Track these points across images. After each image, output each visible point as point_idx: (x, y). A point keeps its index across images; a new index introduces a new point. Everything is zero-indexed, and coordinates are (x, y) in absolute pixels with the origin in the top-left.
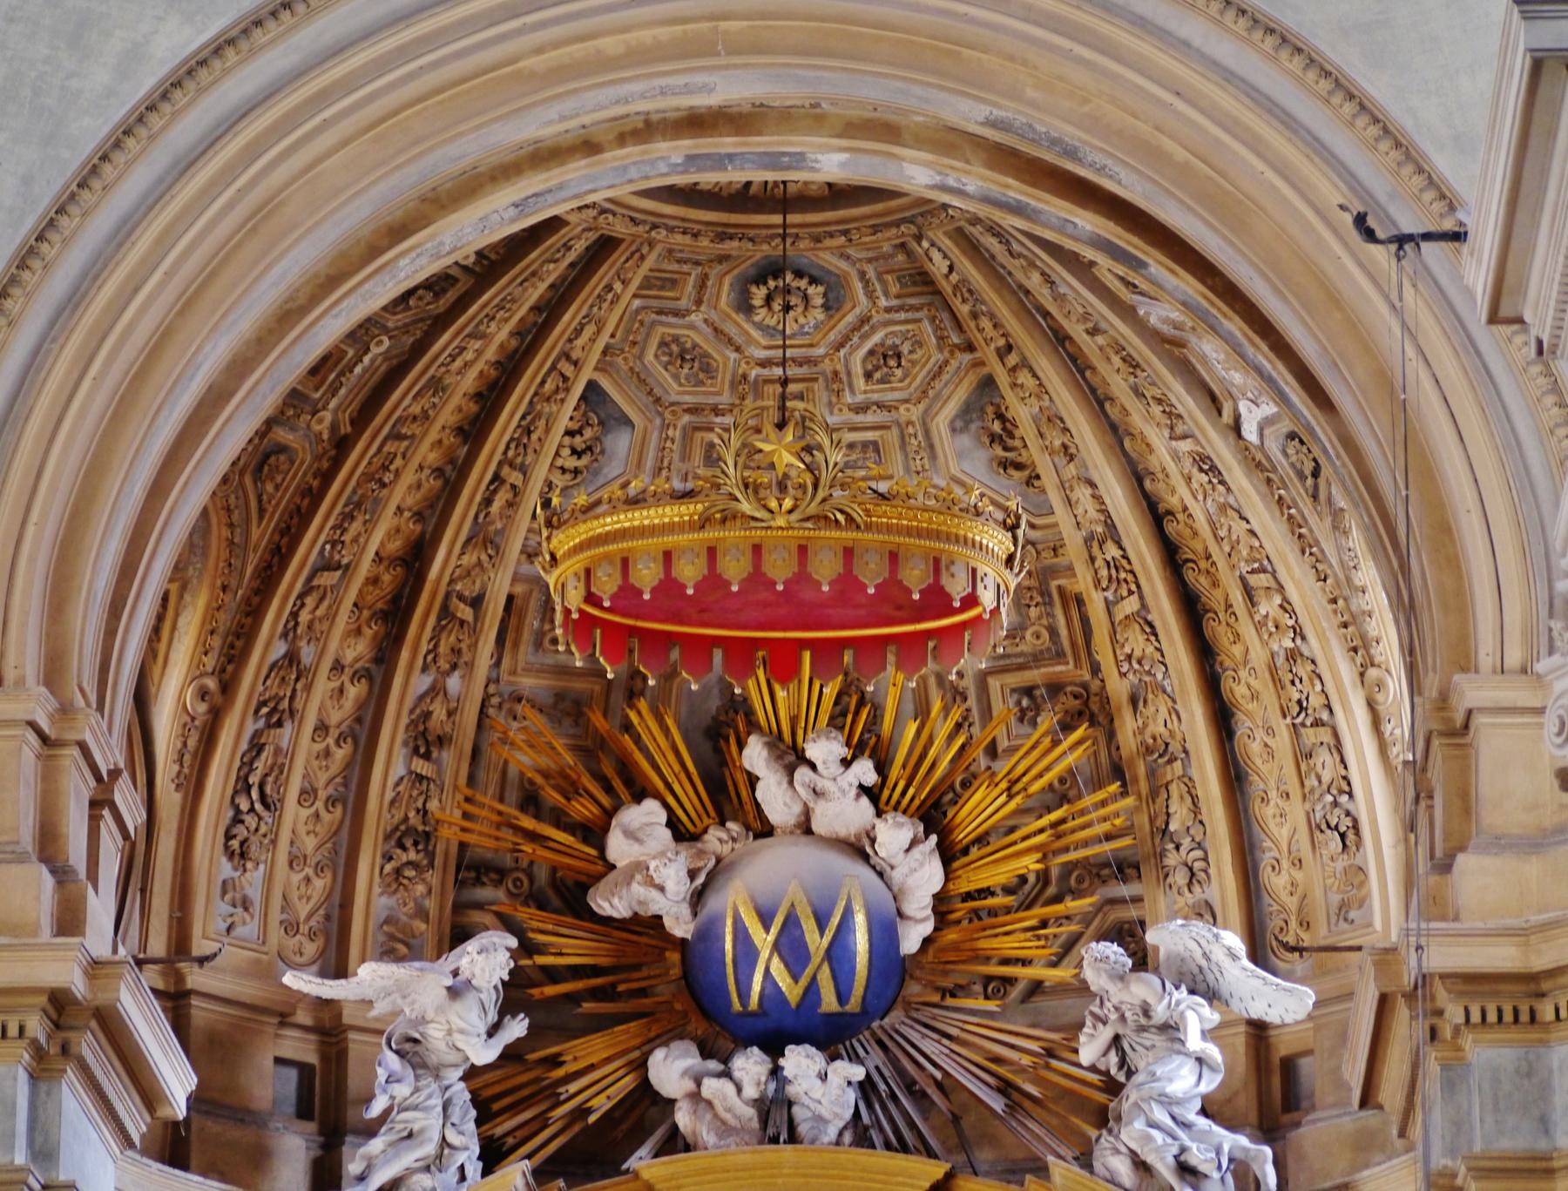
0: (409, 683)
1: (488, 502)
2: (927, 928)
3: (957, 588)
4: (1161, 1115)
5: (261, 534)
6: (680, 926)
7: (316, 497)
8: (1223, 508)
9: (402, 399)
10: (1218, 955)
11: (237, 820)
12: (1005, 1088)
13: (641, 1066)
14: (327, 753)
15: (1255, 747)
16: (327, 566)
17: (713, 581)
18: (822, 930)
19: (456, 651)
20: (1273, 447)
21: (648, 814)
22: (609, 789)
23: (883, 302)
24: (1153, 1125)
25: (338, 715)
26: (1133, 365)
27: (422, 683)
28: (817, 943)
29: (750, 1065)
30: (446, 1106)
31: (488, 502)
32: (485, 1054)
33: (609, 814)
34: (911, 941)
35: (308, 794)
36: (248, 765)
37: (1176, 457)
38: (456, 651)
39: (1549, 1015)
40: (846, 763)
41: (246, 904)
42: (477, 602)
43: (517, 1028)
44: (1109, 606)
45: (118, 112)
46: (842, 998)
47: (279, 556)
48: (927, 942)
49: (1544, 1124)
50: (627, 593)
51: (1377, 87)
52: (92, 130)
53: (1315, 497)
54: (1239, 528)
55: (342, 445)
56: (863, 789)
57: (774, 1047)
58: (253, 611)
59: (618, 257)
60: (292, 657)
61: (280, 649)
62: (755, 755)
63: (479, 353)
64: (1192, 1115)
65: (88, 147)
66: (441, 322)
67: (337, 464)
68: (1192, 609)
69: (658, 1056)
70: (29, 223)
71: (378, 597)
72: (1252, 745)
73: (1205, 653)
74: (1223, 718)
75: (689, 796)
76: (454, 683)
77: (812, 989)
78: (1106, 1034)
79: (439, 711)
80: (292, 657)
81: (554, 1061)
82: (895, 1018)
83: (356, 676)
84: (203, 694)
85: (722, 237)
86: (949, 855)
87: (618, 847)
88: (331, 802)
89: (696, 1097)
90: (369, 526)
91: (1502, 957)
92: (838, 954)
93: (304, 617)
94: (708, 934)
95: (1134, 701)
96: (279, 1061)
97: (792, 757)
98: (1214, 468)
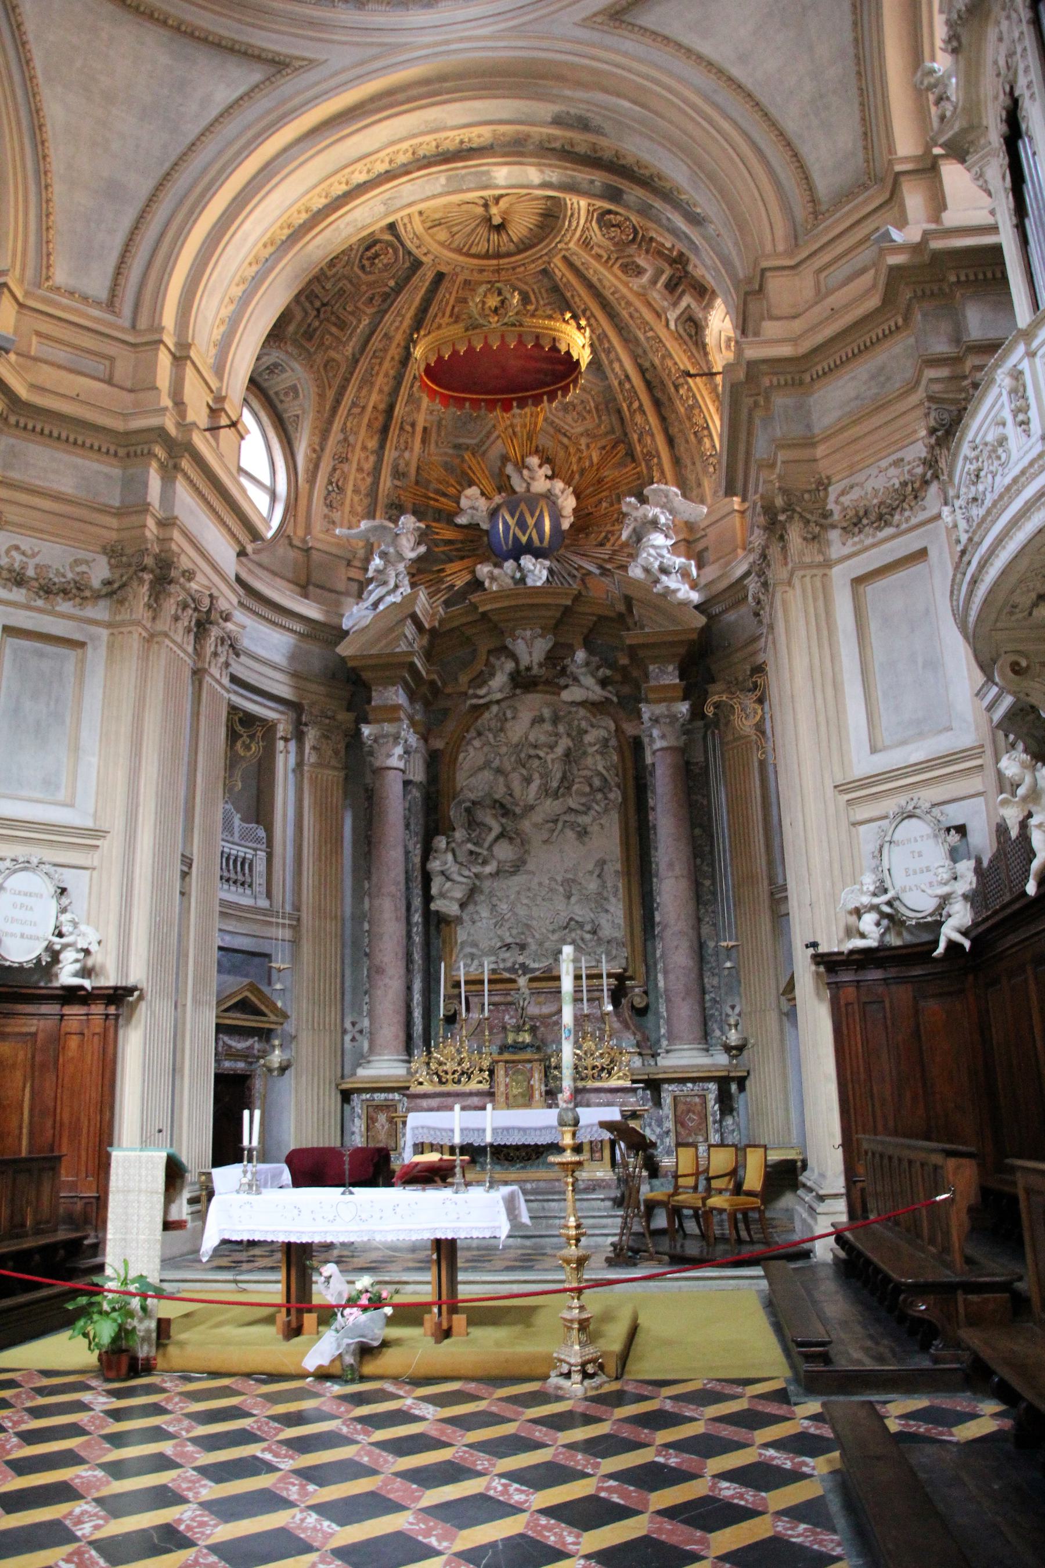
0: (390, 454)
1: (412, 387)
2: (572, 519)
3: (563, 349)
4: (652, 551)
5: (331, 394)
6: (485, 526)
7: (347, 380)
8: (663, 357)
9: (375, 343)
10: (671, 494)
11: (329, 493)
12: (600, 567)
13: (473, 572)
14: (363, 479)
15: (682, 449)
16: (354, 404)
17: (471, 349)
18: (532, 516)
19: (407, 443)
20: (681, 331)
21: (473, 491)
22: (461, 485)
23: (542, 303)
24: (649, 555)
25: (368, 466)
26: (629, 304)
27: (395, 454)
28: (531, 522)
29: (509, 565)
30: (397, 575)
31: (412, 387)
32: (412, 555)
33: (460, 492)
34: (566, 525)
35: (356, 491)
36: (331, 474)
37: (648, 339)
38: (407, 443)
39: (808, 379)
40: (540, 466)
41: (334, 523)
42: (413, 425)
43: (422, 549)
44: (629, 407)
45: (204, 123)
46: (541, 540)
47: (338, 402)
48: (572, 526)
49: (809, 427)
50: (440, 358)
51: (705, 48)
52: (192, 131)
53: (696, 344)
54: (670, 363)
55: (356, 361)
56: (547, 477)
57: (517, 559)
58: (330, 422)
59: (445, 284)
60: (346, 440)
61: (341, 436)
62: (509, 469)
63: (401, 322)
64: (665, 552)
65: (191, 137)
66: (386, 311)
67: (355, 368)
68: (657, 404)
69: (479, 566)
70: (167, 165)
71: (378, 425)
72: (681, 447)
73: (663, 419)
74: (671, 441)
75: (489, 487)
76: (407, 455)
77: (530, 538)
78: (630, 528)
79: (402, 462)
80: (346, 440)
81: (443, 570)
82: (562, 551)
83: (372, 452)
84: (314, 451)
85: (481, 271)
86: (577, 495)
87: (464, 503)
88: (367, 495)
89: (493, 578)
90: (370, 392)
91: (785, 351)
92: (539, 525)
93: (349, 424)
94: (495, 526)
95: (639, 441)
96: (350, 579)
97: (521, 466)
98: (661, 341)
